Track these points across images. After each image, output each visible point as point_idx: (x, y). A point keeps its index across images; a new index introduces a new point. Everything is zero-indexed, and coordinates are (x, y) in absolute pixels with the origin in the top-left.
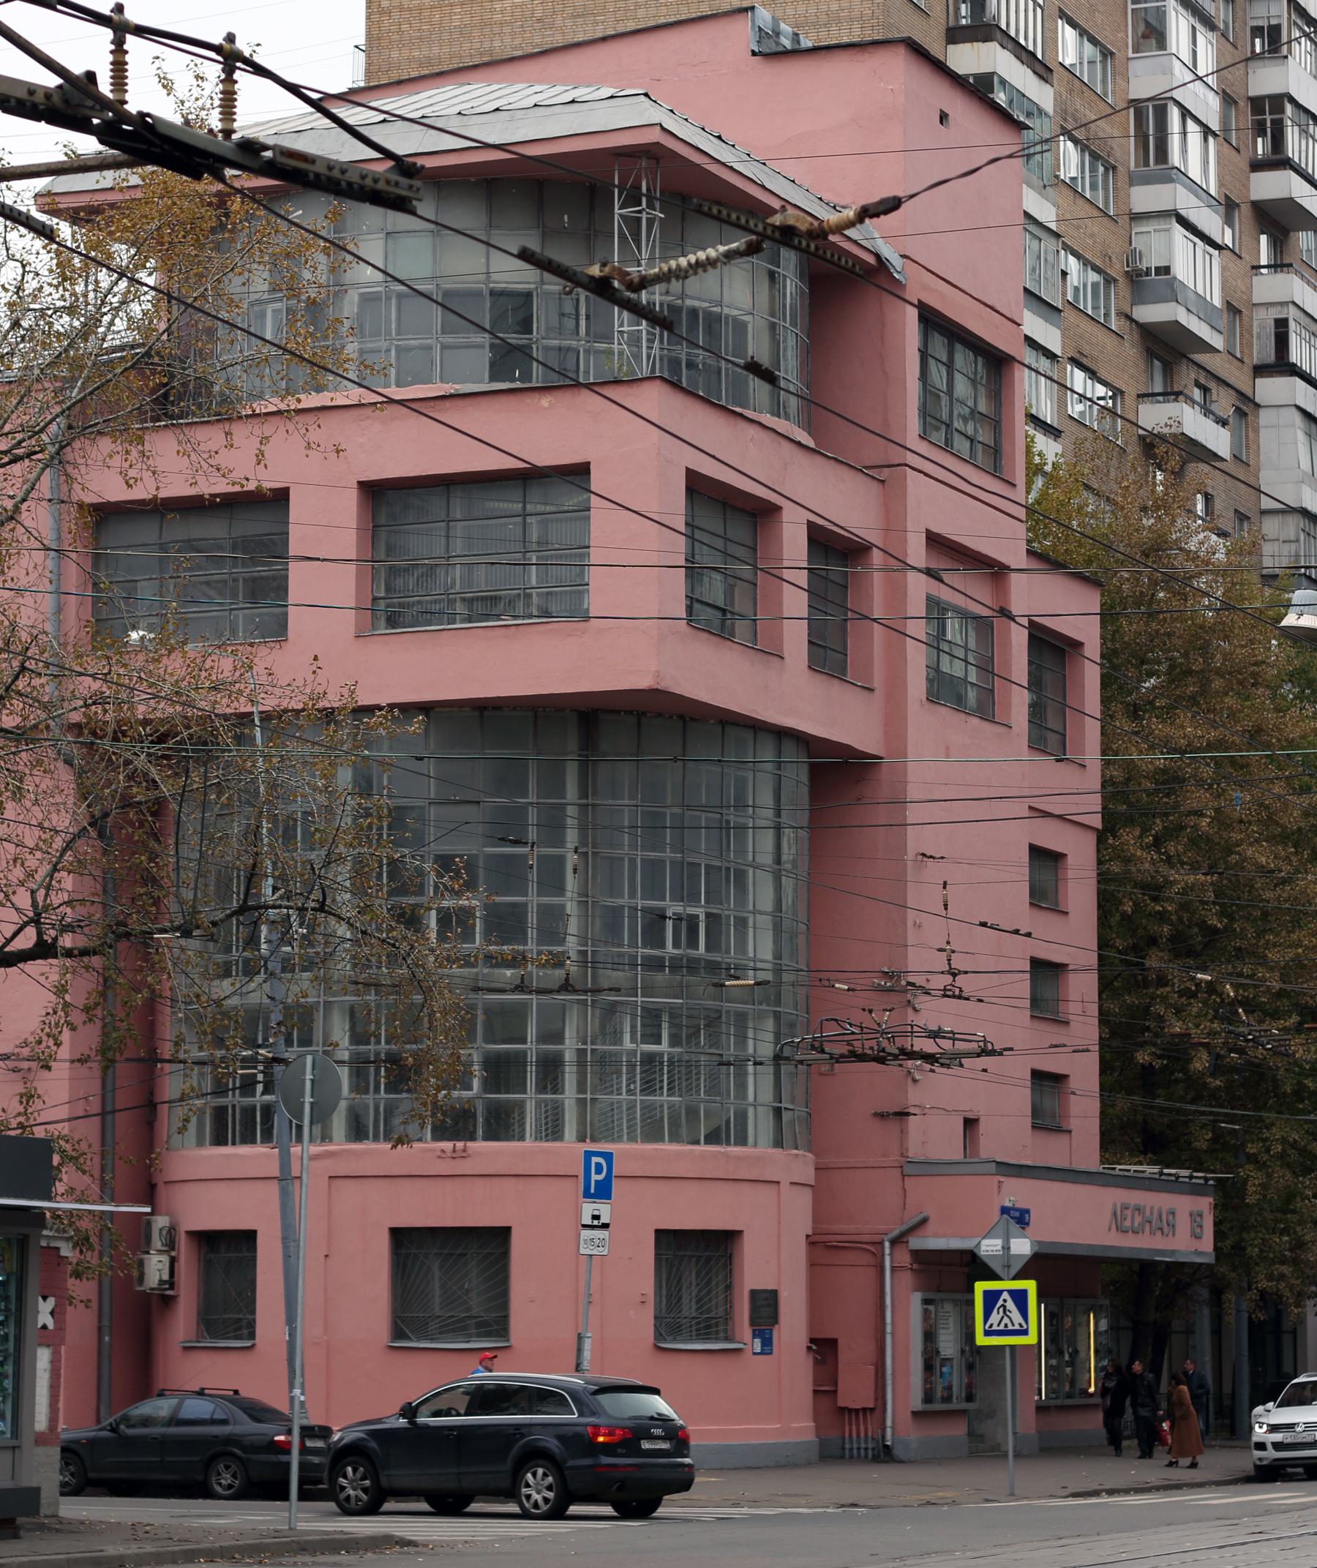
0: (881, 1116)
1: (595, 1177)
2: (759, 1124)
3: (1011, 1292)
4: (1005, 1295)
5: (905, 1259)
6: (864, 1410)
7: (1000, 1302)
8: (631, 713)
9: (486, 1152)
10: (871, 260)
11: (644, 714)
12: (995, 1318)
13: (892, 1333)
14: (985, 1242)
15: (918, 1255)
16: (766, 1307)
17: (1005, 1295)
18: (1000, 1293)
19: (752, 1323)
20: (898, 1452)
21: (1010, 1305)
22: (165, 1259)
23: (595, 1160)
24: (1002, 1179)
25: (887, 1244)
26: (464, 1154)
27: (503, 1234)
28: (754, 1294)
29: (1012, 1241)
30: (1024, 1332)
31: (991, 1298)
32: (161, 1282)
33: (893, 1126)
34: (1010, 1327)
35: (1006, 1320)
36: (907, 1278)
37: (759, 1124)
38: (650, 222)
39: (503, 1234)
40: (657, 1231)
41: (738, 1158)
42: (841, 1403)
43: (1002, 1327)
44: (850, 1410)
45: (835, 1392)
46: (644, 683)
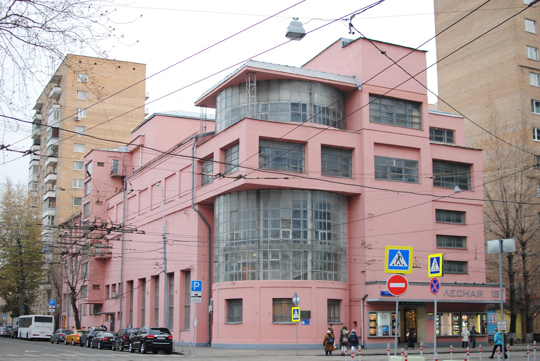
1: (195, 286)
5: (365, 304)
8: (266, 189)
9: (240, 283)
10: (355, 86)
15: (368, 303)
16: (306, 316)
23: (195, 283)
26: (234, 284)
27: (241, 299)
31: (294, 310)
36: (365, 308)
38: (252, 87)
39: (241, 299)
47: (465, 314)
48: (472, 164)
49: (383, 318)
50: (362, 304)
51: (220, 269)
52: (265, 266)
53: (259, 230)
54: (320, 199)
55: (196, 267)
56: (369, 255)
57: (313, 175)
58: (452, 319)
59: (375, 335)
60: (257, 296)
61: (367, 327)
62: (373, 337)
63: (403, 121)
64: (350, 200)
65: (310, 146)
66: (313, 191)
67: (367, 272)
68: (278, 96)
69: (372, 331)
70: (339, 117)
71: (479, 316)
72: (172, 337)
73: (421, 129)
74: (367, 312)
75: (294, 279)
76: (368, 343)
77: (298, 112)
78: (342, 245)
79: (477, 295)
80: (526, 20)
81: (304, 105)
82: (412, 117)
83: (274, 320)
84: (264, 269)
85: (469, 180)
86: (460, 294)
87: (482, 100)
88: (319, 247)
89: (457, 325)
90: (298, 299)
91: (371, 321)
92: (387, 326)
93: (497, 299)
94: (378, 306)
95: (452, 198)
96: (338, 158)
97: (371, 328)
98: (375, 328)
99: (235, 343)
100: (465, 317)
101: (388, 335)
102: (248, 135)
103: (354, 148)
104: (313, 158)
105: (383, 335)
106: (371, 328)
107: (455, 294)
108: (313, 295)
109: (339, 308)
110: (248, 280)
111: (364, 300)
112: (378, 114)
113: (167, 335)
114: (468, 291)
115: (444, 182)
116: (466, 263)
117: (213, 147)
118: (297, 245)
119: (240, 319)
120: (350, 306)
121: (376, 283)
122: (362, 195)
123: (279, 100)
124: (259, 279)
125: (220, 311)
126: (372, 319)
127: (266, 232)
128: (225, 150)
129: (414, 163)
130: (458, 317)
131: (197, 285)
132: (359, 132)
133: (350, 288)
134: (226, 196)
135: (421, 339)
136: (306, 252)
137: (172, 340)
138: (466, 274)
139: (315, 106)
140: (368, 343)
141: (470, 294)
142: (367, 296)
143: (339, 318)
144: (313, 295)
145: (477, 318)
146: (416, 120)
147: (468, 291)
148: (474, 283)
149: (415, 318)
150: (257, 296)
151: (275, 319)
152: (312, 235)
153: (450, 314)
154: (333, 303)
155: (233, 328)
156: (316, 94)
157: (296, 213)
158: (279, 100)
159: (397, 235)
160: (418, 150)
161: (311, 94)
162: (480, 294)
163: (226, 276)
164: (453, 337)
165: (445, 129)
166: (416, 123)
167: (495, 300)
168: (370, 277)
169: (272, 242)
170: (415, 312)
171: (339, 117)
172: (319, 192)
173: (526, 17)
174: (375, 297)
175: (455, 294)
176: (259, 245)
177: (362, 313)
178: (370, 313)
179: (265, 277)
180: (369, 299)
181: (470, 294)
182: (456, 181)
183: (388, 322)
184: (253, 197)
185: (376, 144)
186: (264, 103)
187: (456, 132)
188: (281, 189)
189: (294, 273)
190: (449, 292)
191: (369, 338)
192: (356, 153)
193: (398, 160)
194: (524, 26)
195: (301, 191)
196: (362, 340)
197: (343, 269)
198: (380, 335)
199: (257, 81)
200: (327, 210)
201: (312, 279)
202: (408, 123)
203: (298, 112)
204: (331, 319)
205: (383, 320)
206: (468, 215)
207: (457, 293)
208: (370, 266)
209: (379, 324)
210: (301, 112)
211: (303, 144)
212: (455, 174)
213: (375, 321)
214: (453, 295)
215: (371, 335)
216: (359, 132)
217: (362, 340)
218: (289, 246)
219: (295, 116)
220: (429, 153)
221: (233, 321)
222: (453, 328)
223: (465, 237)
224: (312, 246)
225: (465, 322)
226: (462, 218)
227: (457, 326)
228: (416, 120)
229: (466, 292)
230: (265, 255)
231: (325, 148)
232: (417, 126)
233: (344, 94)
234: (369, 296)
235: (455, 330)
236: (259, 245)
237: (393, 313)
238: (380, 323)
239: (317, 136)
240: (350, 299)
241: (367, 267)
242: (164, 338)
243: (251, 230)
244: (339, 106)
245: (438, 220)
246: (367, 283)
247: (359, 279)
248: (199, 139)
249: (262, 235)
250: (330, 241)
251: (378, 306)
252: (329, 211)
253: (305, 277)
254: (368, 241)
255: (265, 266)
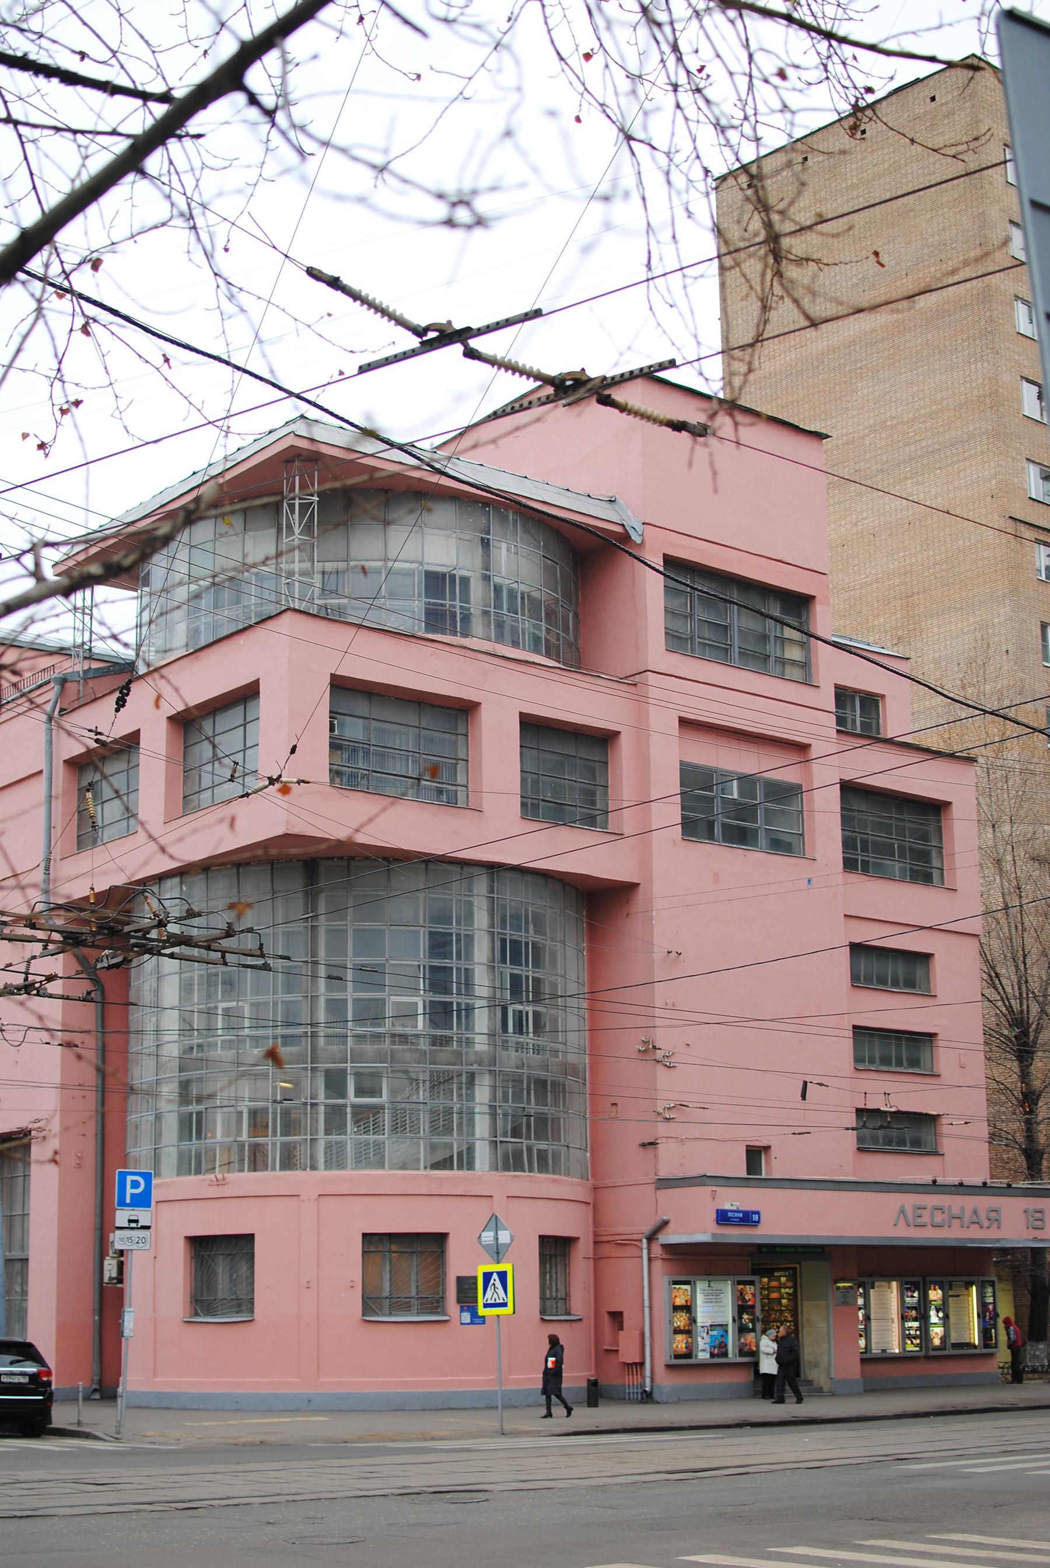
0: (643, 1145)
1: (129, 1191)
2: (482, 1153)
3: (498, 1273)
4: (495, 1276)
5: (657, 1251)
6: (636, 1364)
7: (492, 1282)
8: (342, 858)
11: (353, 858)
12: (489, 1292)
13: (651, 1308)
14: (484, 1234)
15: (669, 1248)
17: (495, 1276)
18: (491, 1274)
19: (459, 1301)
20: (656, 1396)
21: (498, 1284)
22: (114, 1262)
23: (129, 1178)
24: (714, 1188)
25: (644, 1241)
26: (221, 1183)
27: (250, 1238)
28: (460, 1280)
29: (499, 1232)
30: (505, 1305)
32: (111, 1279)
33: (650, 1151)
34: (498, 1301)
35: (495, 1295)
36: (658, 1265)
37: (482, 1153)
38: (304, 507)
39: (250, 1238)
40: (364, 1235)
41: (441, 1179)
42: (621, 1359)
43: (493, 1302)
44: (628, 1364)
45: (617, 1351)
46: (280, 831)
47: (935, 1283)
48: (948, 804)
49: (714, 1298)
50: (645, 1252)
51: (154, 1128)
52: (335, 1120)
53: (314, 998)
54: (518, 896)
55: (55, 1126)
56: (669, 1086)
57: (493, 821)
58: (903, 1301)
59: (688, 1355)
60: (311, 1227)
61: (663, 1330)
62: (683, 1362)
63: (758, 657)
64: (599, 903)
65: (486, 717)
66: (493, 868)
67: (662, 1148)
68: (381, 545)
69: (680, 1343)
70: (566, 630)
71: (974, 1288)
72: (49, 1373)
73: (808, 682)
74: (662, 1281)
75: (436, 1166)
76: (666, 1382)
77: (442, 605)
78: (572, 1058)
79: (986, 1223)
80: (1025, 383)
81: (465, 581)
82: (782, 641)
83: (367, 1309)
84: (328, 1131)
85: (934, 854)
86: (939, 1218)
87: (882, 620)
88: (510, 1059)
89: (915, 1319)
90: (504, 1237)
91: (676, 1308)
92: (724, 1327)
93: (1039, 1234)
94: (695, 1261)
95: (894, 907)
96: (569, 761)
97: (677, 1331)
98: (688, 1332)
99: (225, 1391)
100: (935, 1295)
101: (725, 1354)
102: (291, 668)
103: (617, 734)
104: (497, 757)
105: (712, 1355)
106: (677, 1331)
107: (926, 1219)
108: (498, 1224)
109: (566, 1265)
110: (273, 1169)
111: (651, 1238)
112: (685, 628)
113: (32, 1369)
114: (963, 1209)
115: (871, 858)
116: (933, 1119)
117: (146, 715)
118: (444, 1053)
119: (244, 1304)
120: (597, 1260)
121: (703, 1180)
122: (641, 891)
123: (386, 560)
124: (313, 1168)
125: (157, 1280)
126: (679, 1302)
127: (336, 1007)
128: (186, 723)
129: (785, 794)
130: (916, 1294)
131: (135, 1184)
132: (633, 681)
133: (596, 1200)
134: (188, 879)
135: (816, 1365)
136: (472, 1076)
137: (49, 1383)
138: (935, 1153)
139: (498, 589)
140: (666, 1382)
141: (967, 1220)
142: (665, 1223)
143: (566, 1299)
144: (498, 1224)
145: (969, 1295)
146: (794, 653)
147: (963, 1209)
148: (961, 1185)
149: (794, 1298)
150: (311, 1227)
151: (371, 1304)
152: (491, 1018)
153: (894, 1284)
154: (555, 1249)
155: (214, 1339)
156: (504, 546)
157: (440, 944)
158: (386, 560)
159: (748, 1020)
160: (802, 748)
161: (485, 544)
162: (995, 1218)
163: (181, 1155)
164: (903, 1359)
165: (857, 691)
166: (793, 663)
167: (1035, 1239)
168: (671, 1161)
169: (360, 1038)
170: (793, 1278)
171: (566, 630)
172: (509, 874)
173: (1025, 373)
174: (701, 1230)
175: (926, 1219)
176: (314, 1049)
177: (647, 1289)
178: (675, 1283)
179: (335, 1159)
180: (672, 1237)
181: (967, 1220)
182: (902, 855)
183: (727, 1313)
184: (296, 883)
185: (685, 723)
186: (329, 566)
187: (887, 699)
188: (392, 859)
189: (433, 1148)
190: (909, 1212)
191: (669, 1367)
192: (626, 745)
193: (747, 781)
194: (1019, 401)
195: (458, 869)
196: (648, 1373)
197: (575, 1132)
198: (703, 1356)
199: (316, 490)
200: (532, 936)
201: (494, 1167)
202: (772, 660)
203: (442, 605)
204: (553, 1302)
205: (714, 1305)
206: (939, 966)
207: (932, 1217)
208: (671, 1124)
209: (699, 1320)
210: (458, 603)
211: (462, 711)
212: (895, 832)
213: (688, 1308)
214: (919, 1221)
215: (677, 1357)
216: (633, 681)
217: (648, 1373)
218: (415, 1055)
219: (438, 619)
220: (837, 761)
221: (208, 1313)
222: (903, 1329)
223: (932, 1036)
224: (493, 1061)
225: (938, 1310)
226: (919, 973)
227: (916, 1324)
228: (794, 653)
229: (955, 1211)
230: (335, 1083)
231: (534, 728)
232: (795, 673)
233: (583, 553)
234: (671, 1225)
235: (909, 1337)
236: (314, 1049)
237: (740, 1283)
238: (703, 1315)
239: (508, 688)
240: (595, 1235)
241: (663, 1129)
242: (24, 1380)
243: (281, 996)
244: (566, 595)
245: (857, 980)
246: (665, 1183)
247: (628, 1166)
248: (71, 687)
249: (322, 1016)
250: (542, 1041)
251: (695, 1261)
252: (538, 939)
253: (466, 1160)
254: (664, 1039)
255: (335, 1120)
